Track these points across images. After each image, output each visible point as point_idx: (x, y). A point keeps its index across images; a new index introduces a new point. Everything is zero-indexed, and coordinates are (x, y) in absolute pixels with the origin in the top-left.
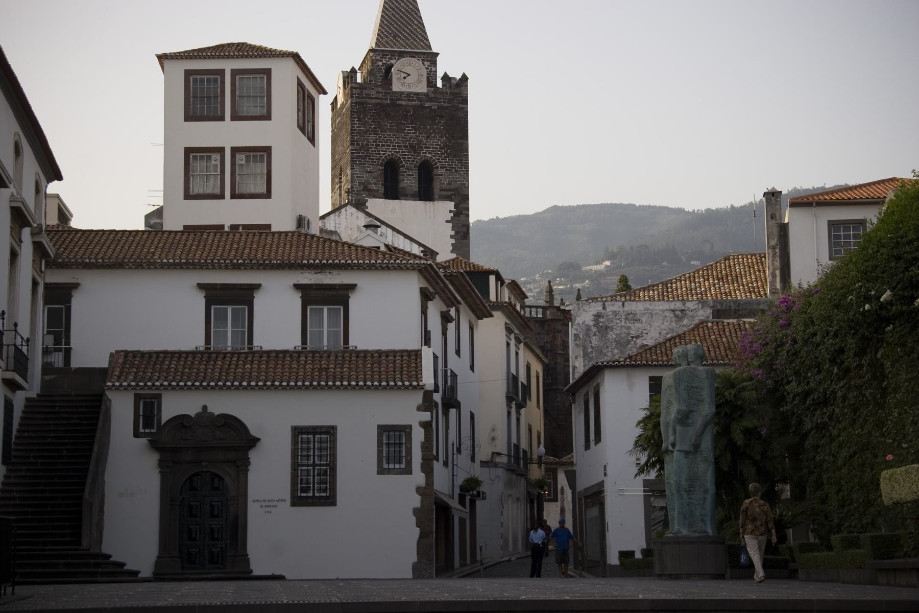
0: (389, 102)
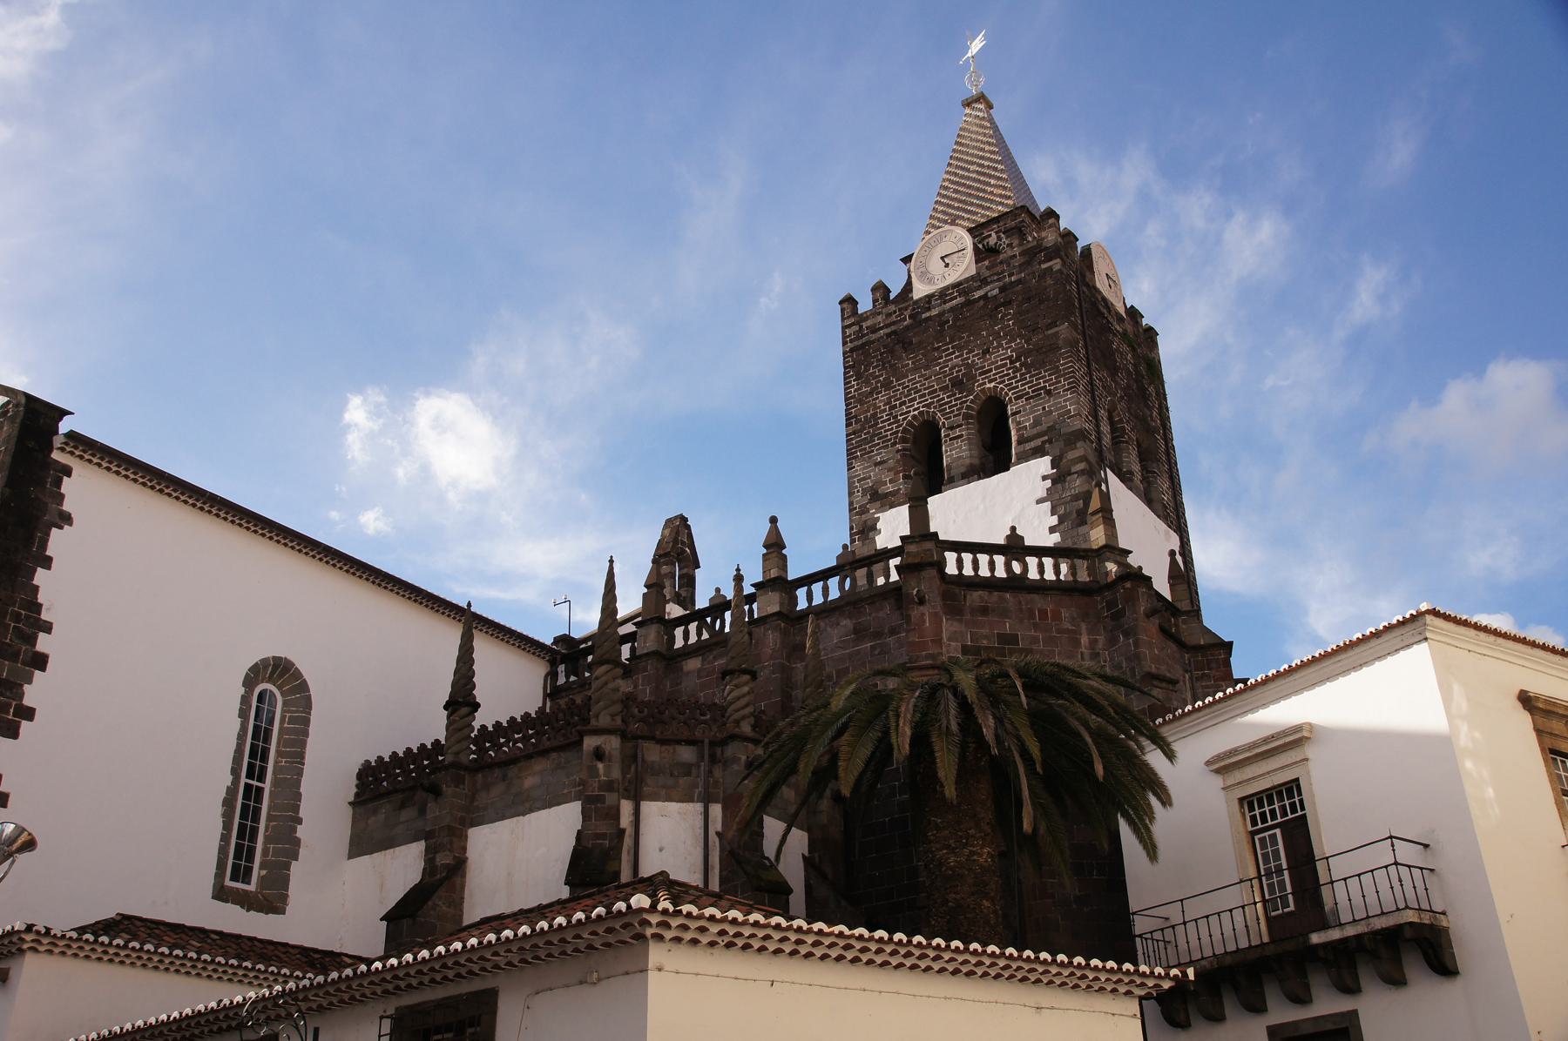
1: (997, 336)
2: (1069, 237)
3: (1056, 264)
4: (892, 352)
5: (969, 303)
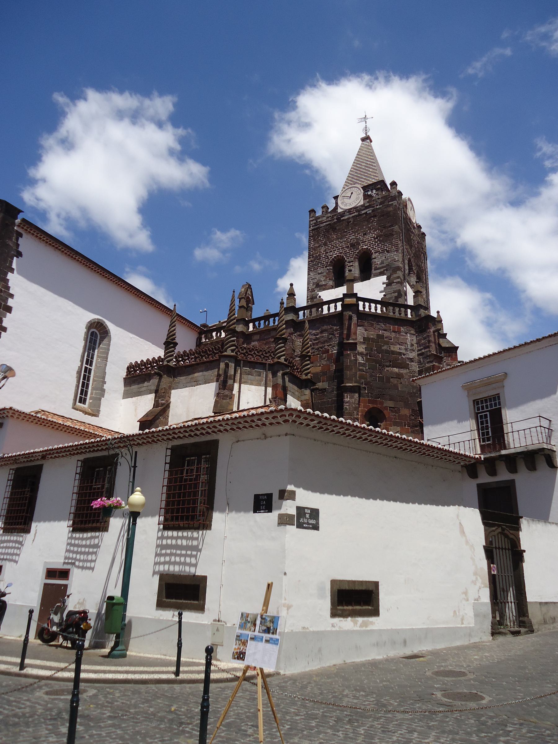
0: (335, 220)
1: (370, 229)
2: (400, 194)
3: (395, 203)
4: (328, 232)
5: (360, 215)
